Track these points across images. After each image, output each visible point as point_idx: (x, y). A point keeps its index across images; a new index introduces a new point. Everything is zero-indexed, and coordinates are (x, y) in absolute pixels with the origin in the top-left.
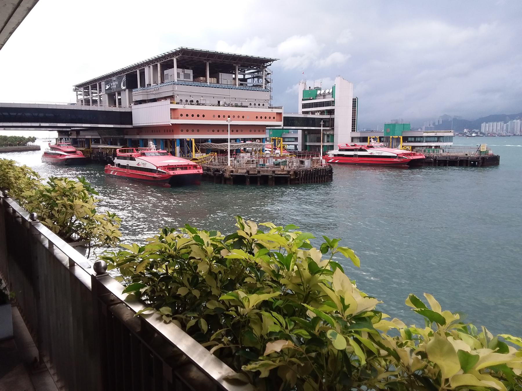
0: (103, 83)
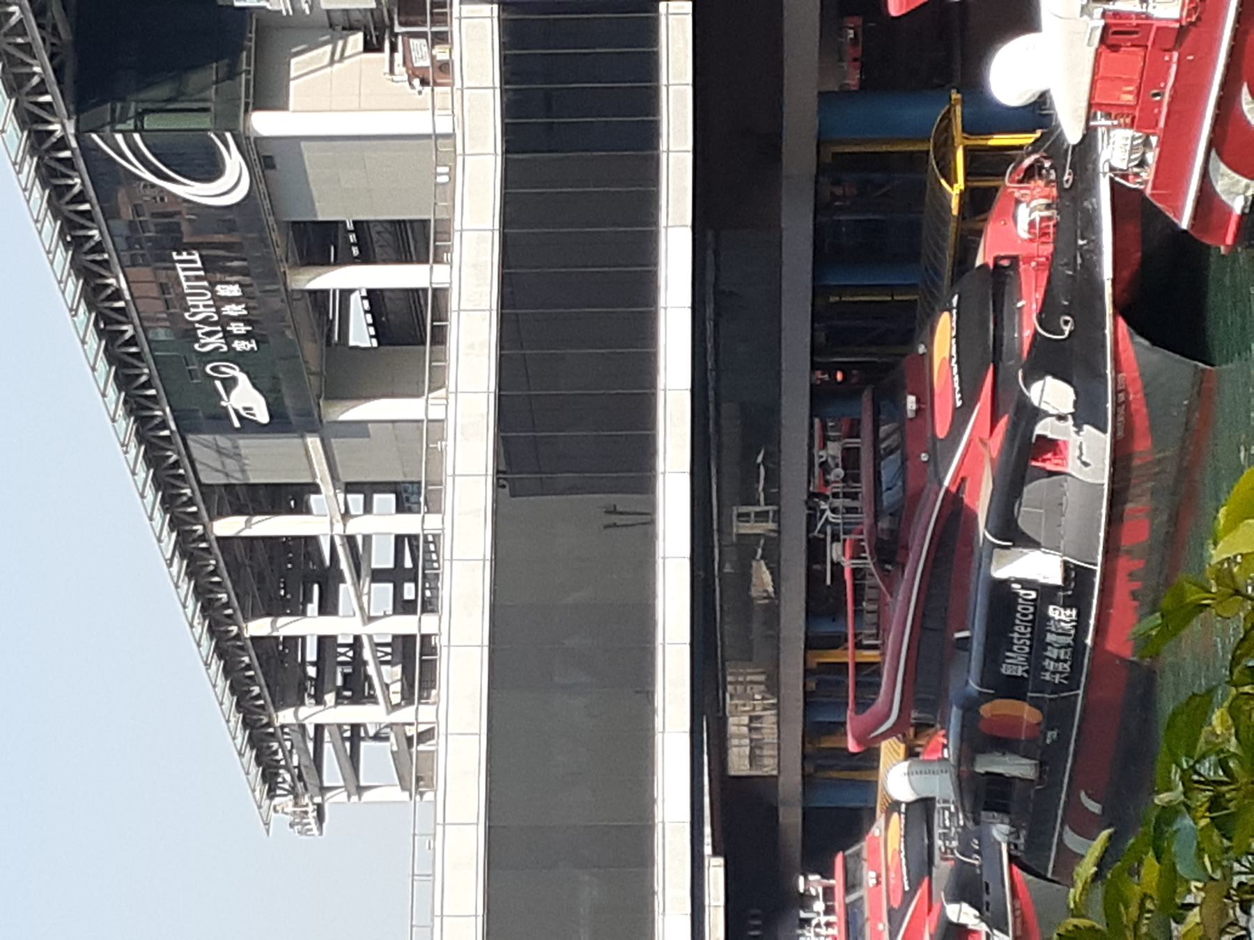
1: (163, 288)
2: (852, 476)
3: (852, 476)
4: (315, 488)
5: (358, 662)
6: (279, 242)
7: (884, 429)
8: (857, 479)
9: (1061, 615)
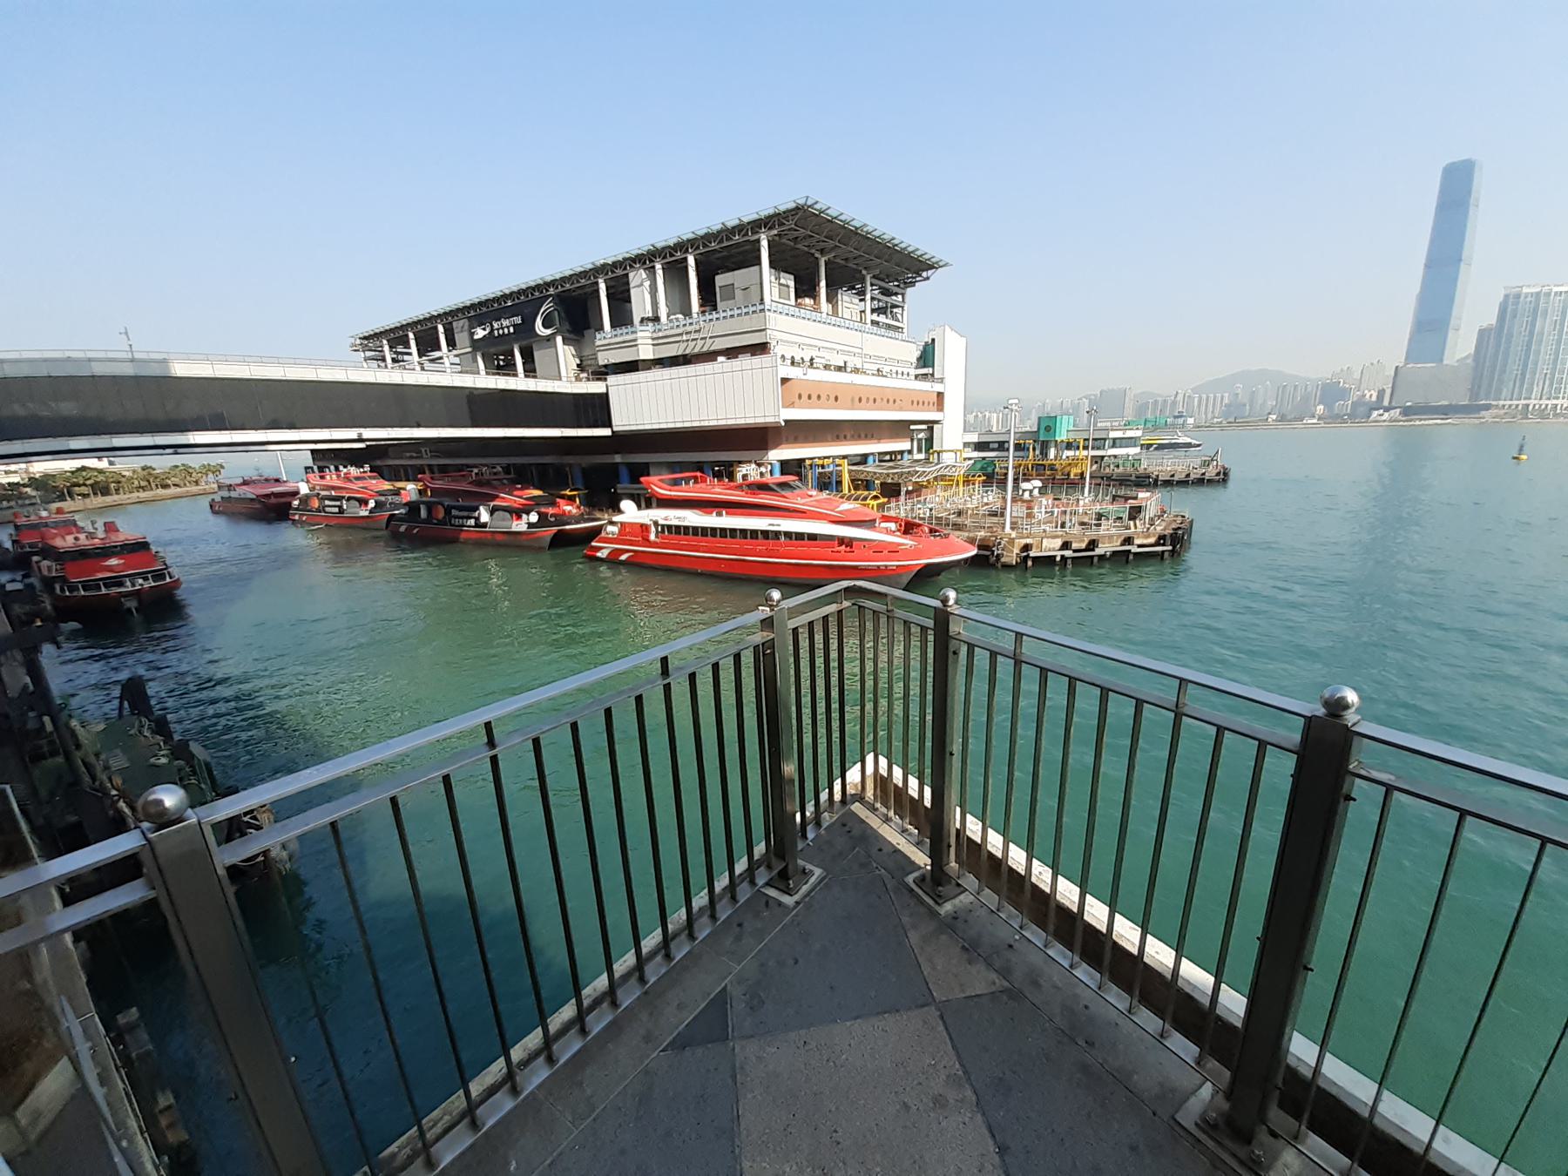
0: (460, 325)
9: (472, 522)
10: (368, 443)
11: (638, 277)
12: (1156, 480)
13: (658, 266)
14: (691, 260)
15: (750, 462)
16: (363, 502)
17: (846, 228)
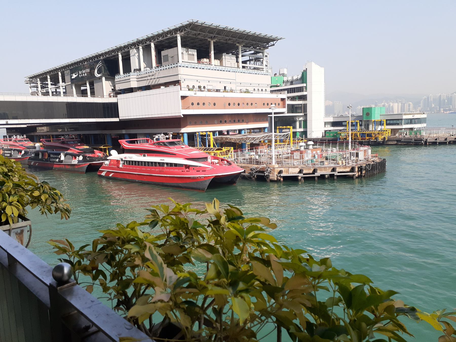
0: (67, 72)
1: (85, 68)
2: (71, 139)
3: (71, 139)
4: (65, 83)
5: (46, 88)
6: (91, 80)
7: (76, 142)
8: (71, 139)
9: (57, 160)
10: (27, 125)
11: (133, 52)
12: (426, 142)
13: (140, 47)
14: (153, 45)
15: (162, 133)
16: (20, 151)
17: (217, 29)
